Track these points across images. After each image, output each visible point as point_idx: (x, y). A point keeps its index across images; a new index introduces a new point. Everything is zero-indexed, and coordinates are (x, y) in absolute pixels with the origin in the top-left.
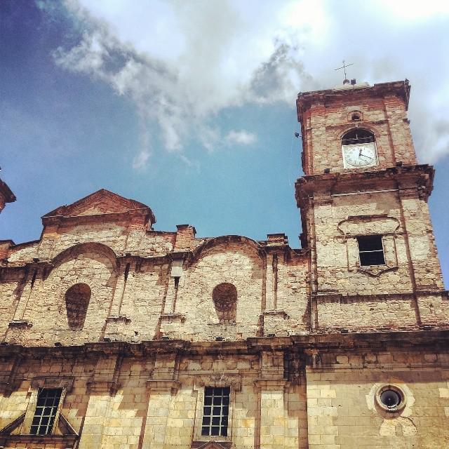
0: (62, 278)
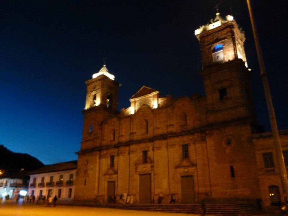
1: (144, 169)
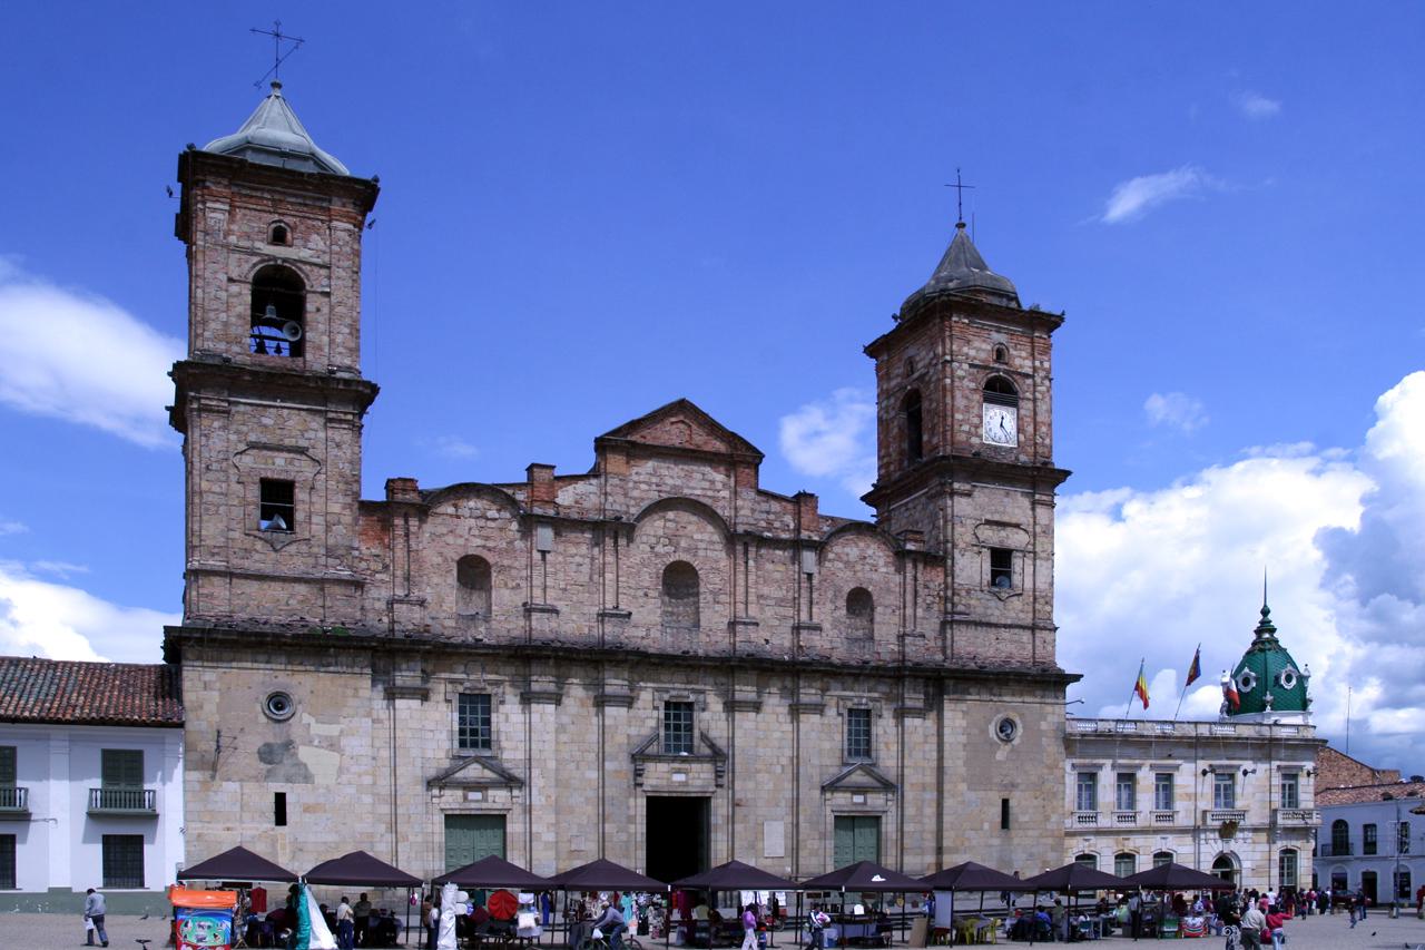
0: (652, 548)
1: (680, 778)
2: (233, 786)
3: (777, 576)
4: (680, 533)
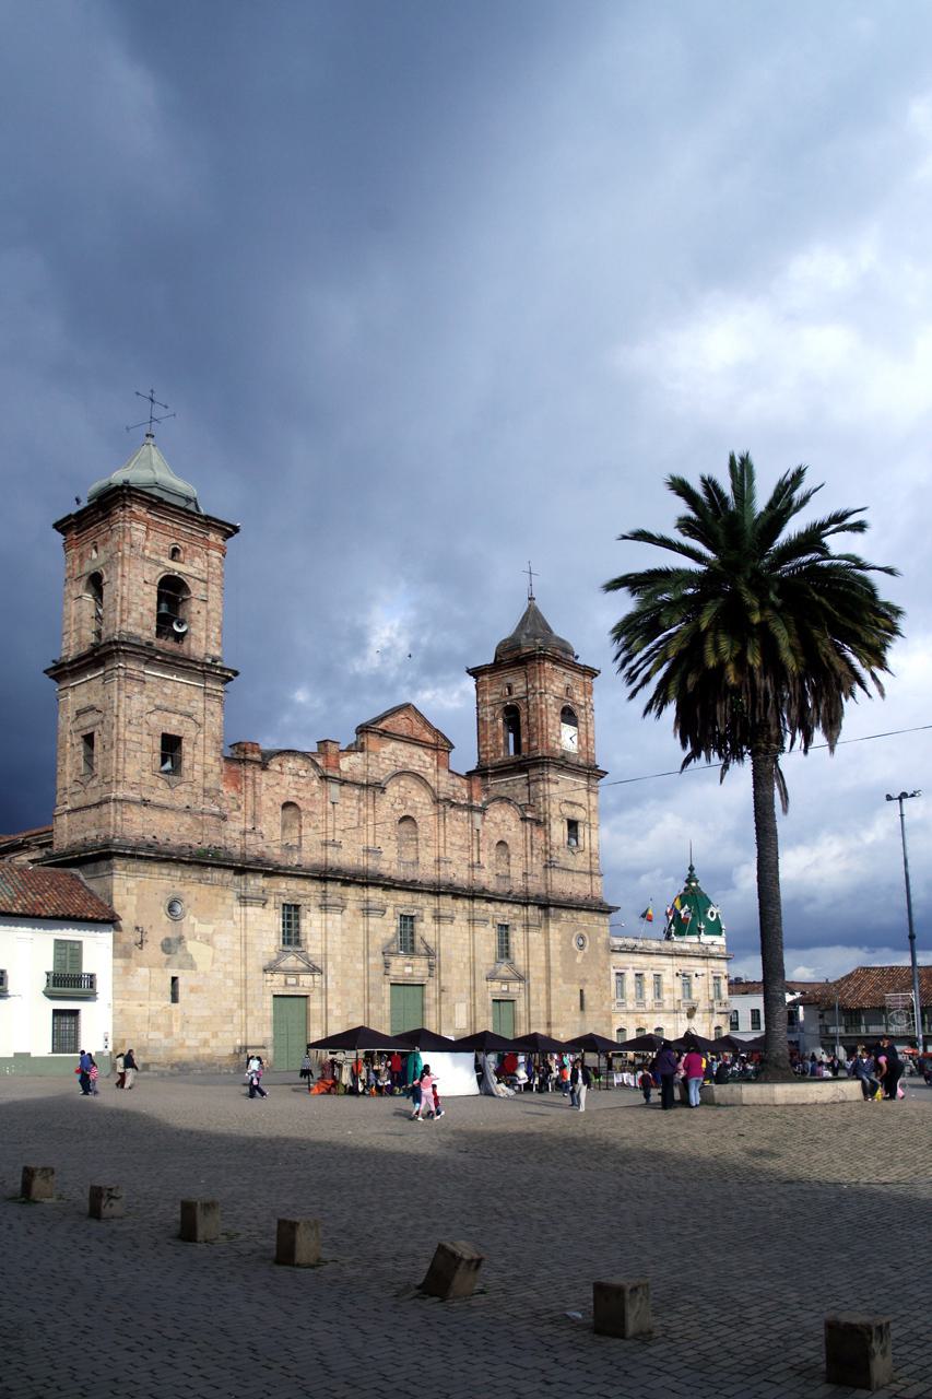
1: (408, 970)
2: (143, 971)
3: (459, 829)
4: (408, 795)
